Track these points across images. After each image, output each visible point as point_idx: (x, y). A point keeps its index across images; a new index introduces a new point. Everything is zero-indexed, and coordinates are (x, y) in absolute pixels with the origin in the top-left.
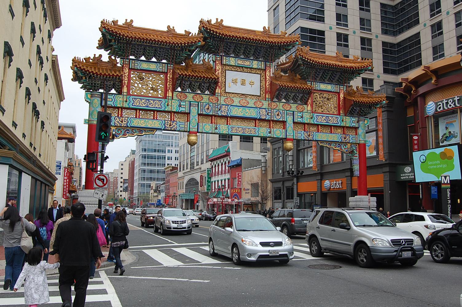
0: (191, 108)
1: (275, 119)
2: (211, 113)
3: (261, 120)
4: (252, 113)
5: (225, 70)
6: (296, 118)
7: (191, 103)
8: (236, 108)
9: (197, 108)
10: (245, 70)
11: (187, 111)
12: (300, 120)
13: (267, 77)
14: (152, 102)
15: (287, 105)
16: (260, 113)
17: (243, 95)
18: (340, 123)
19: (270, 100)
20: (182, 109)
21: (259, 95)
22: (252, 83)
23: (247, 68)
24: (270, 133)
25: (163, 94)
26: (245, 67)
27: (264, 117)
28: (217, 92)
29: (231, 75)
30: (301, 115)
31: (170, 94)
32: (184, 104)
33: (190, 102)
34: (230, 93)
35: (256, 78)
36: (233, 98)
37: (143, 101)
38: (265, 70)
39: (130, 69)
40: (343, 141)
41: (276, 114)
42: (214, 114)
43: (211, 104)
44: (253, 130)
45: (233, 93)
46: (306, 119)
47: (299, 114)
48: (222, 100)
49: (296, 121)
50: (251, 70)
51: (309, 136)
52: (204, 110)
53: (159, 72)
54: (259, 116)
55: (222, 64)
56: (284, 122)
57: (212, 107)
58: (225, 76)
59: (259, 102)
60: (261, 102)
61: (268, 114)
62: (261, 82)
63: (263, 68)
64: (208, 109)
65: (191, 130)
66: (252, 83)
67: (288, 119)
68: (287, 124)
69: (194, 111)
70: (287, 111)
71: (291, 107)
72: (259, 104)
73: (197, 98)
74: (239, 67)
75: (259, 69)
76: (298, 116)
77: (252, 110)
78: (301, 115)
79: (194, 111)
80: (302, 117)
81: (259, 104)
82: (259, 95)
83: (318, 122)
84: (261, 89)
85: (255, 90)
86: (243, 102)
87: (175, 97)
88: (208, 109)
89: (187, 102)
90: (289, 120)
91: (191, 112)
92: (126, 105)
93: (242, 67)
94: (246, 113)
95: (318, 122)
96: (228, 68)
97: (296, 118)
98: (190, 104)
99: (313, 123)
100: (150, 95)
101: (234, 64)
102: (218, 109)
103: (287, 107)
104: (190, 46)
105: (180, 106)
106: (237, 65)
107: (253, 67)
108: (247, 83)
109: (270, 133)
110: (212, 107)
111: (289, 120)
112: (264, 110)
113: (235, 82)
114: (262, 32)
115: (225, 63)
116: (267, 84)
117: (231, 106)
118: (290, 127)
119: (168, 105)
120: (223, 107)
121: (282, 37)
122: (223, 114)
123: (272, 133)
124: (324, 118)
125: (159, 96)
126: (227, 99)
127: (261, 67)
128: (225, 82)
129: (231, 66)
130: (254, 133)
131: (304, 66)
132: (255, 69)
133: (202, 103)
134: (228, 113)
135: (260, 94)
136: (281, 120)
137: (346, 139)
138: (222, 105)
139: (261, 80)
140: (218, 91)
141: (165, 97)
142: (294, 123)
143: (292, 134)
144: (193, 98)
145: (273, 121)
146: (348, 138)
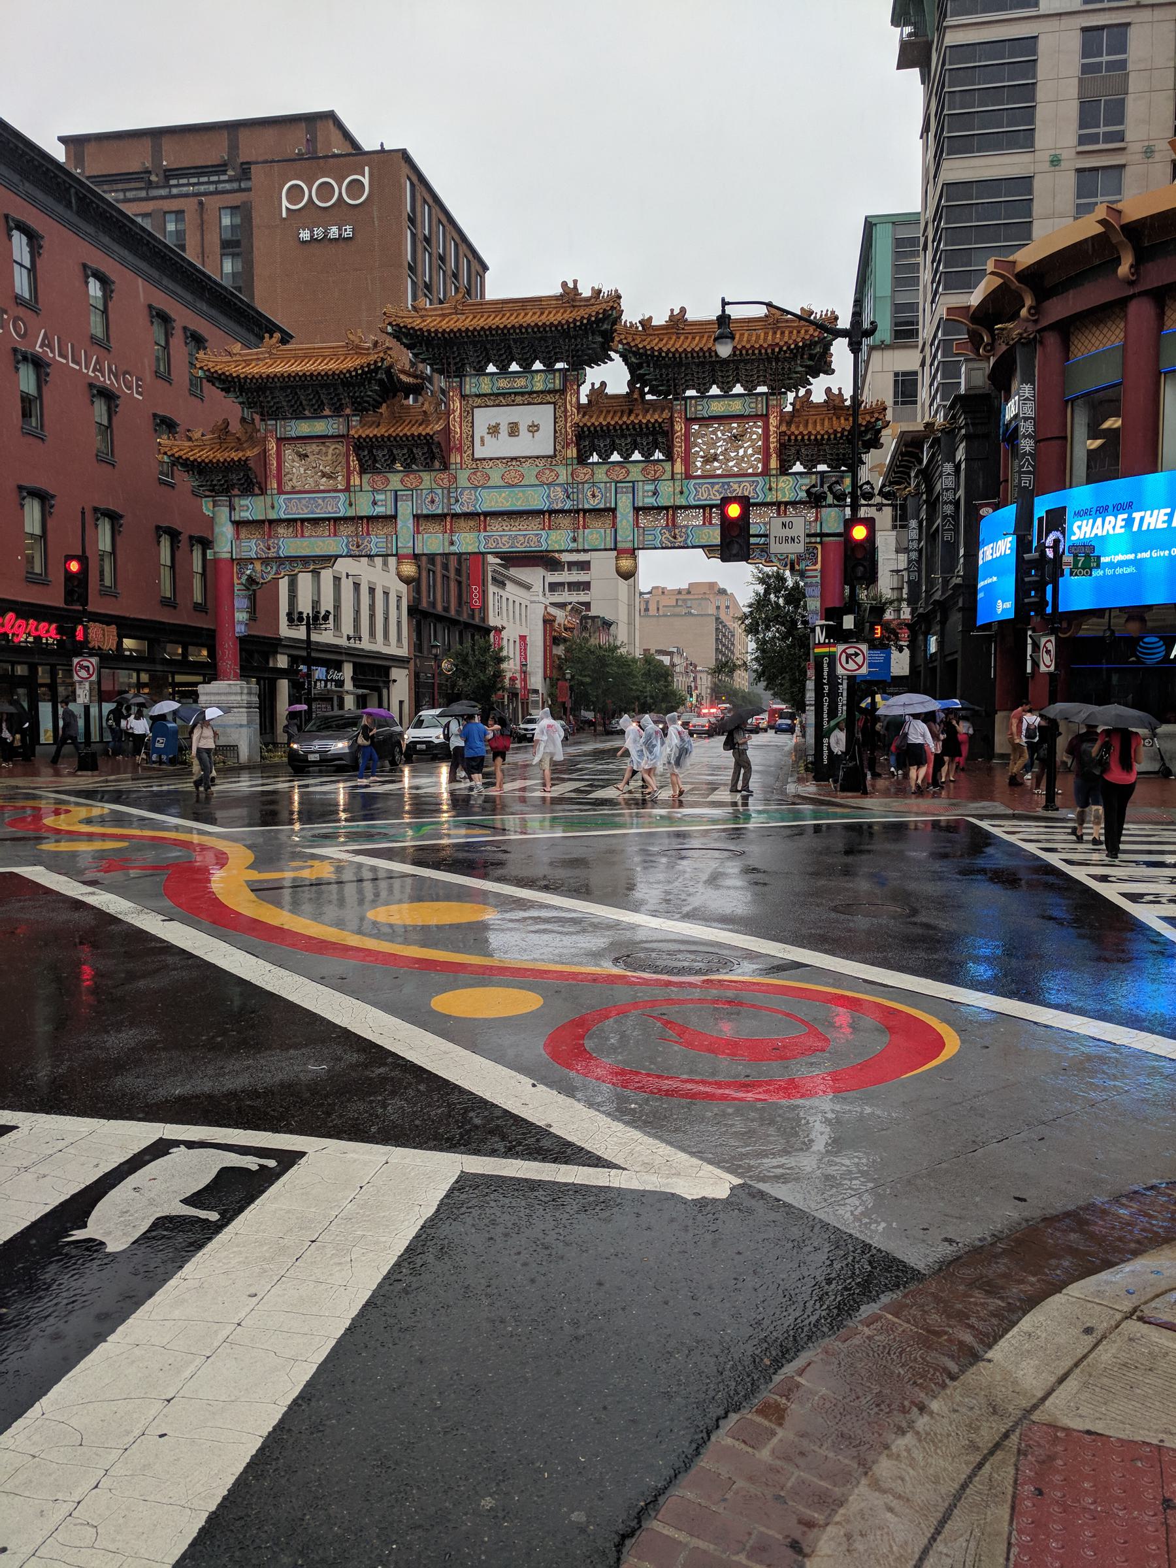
1: (587, 506)
2: (439, 511)
3: (551, 512)
4: (536, 500)
5: (473, 408)
6: (640, 498)
8: (494, 492)
9: (410, 503)
10: (519, 399)
11: (389, 513)
12: (650, 501)
13: (569, 407)
14: (320, 501)
15: (617, 468)
16: (549, 496)
17: (513, 459)
18: (761, 496)
19: (575, 461)
20: (380, 510)
21: (551, 453)
22: (534, 428)
23: (522, 394)
24: (574, 540)
25: (344, 483)
26: (516, 394)
27: (559, 506)
28: (452, 461)
29: (484, 417)
30: (652, 487)
31: (355, 480)
32: (382, 497)
33: (396, 491)
34: (484, 459)
35: (543, 415)
36: (488, 471)
37: (304, 502)
38: (562, 392)
39: (280, 441)
41: (589, 494)
42: (445, 511)
43: (439, 491)
44: (535, 539)
45: (491, 459)
46: (667, 494)
47: (647, 487)
48: (463, 478)
49: (640, 504)
50: (530, 397)
51: (675, 538)
53: (332, 437)
55: (463, 397)
56: (613, 510)
58: (473, 423)
59: (547, 472)
60: (552, 470)
61: (568, 497)
62: (555, 423)
63: (557, 387)
64: (433, 502)
65: (401, 552)
66: (534, 428)
67: (620, 504)
68: (618, 515)
69: (406, 511)
70: (617, 482)
71: (628, 472)
72: (548, 476)
73: (411, 480)
74: (503, 394)
75: (550, 392)
76: (644, 491)
77: (529, 491)
78: (652, 487)
79: (406, 511)
80: (655, 493)
81: (548, 476)
82: (551, 453)
83: (699, 500)
84: (555, 438)
85: (543, 444)
86: (512, 477)
87: (366, 487)
88: (433, 502)
90: (624, 505)
91: (399, 513)
92: (273, 515)
93: (510, 394)
94: (517, 500)
95: (699, 500)
96: (479, 401)
97: (640, 498)
98: (396, 496)
99: (685, 503)
100: (322, 488)
101: (489, 391)
102: (453, 501)
103: (620, 474)
104: (370, 371)
105: (375, 503)
106: (496, 391)
107: (535, 389)
108: (523, 428)
109: (574, 540)
111: (624, 505)
112: (558, 489)
113: (494, 430)
114: (556, 298)
115: (468, 392)
116: (569, 425)
117: (484, 488)
118: (624, 522)
119: (351, 505)
120: (464, 498)
121: (593, 301)
122: (466, 509)
123: (581, 540)
124: (716, 487)
125: (340, 487)
126: (474, 473)
127: (551, 386)
128: (473, 436)
129: (485, 395)
131: (648, 366)
132: (542, 392)
135: (555, 450)
136: (602, 506)
138: (464, 488)
139: (555, 418)
140: (455, 458)
141: (347, 489)
142: (637, 510)
143: (631, 538)
144: (402, 481)
145: (585, 511)
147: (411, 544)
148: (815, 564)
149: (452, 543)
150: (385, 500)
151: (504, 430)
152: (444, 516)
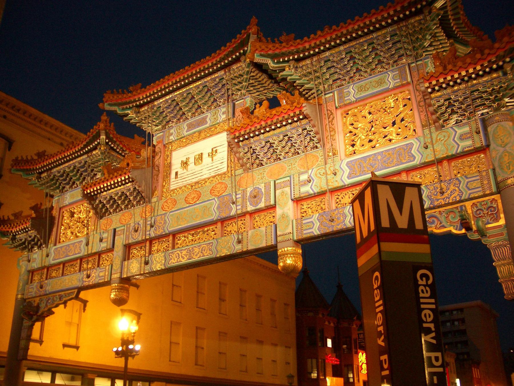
0: (116, 237)
7: (117, 230)
24: (239, 242)
40: (436, 203)
50: (211, 132)
52: (130, 235)
54: (218, 214)
57: (142, 226)
89: (110, 232)
102: (148, 227)
108: (205, 156)
110: (142, 226)
130: (208, 252)
133: (128, 226)
134: (166, 229)
137: (446, 195)
146: (452, 187)
147: (119, 271)
148: (497, 219)
149: (147, 263)
150: (107, 238)
151: (192, 160)
152: (144, 241)
